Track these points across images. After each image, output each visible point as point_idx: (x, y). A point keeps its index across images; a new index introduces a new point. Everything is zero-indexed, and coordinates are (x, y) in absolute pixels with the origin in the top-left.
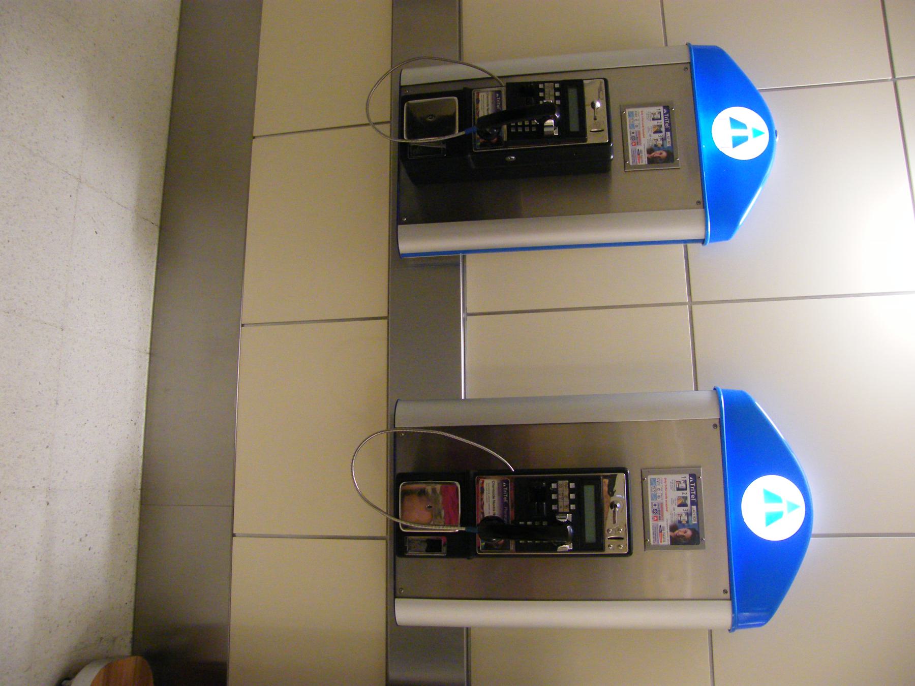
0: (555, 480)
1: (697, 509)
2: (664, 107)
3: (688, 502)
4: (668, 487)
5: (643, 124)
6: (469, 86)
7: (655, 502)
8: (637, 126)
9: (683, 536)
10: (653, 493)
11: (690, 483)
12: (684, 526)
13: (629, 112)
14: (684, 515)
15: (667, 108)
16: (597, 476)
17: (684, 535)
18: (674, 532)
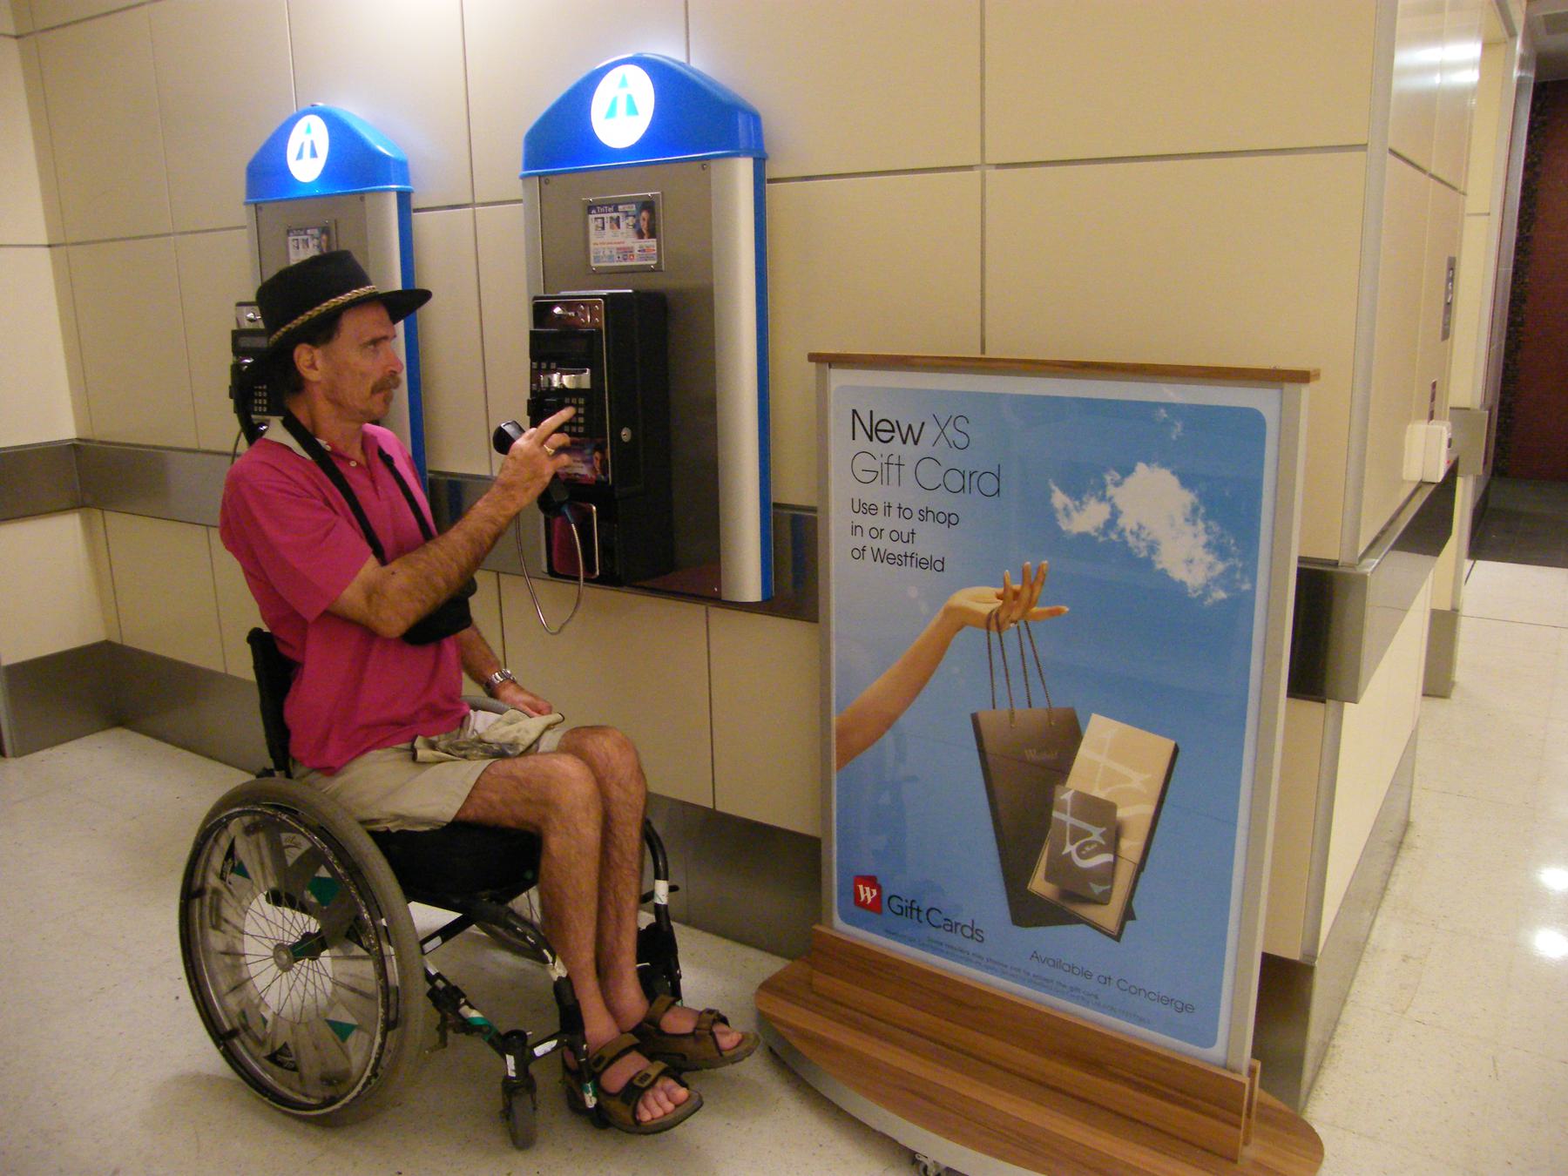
1: (622, 204)
3: (615, 215)
11: (597, 213)
12: (638, 221)
14: (627, 221)
15: (288, 232)
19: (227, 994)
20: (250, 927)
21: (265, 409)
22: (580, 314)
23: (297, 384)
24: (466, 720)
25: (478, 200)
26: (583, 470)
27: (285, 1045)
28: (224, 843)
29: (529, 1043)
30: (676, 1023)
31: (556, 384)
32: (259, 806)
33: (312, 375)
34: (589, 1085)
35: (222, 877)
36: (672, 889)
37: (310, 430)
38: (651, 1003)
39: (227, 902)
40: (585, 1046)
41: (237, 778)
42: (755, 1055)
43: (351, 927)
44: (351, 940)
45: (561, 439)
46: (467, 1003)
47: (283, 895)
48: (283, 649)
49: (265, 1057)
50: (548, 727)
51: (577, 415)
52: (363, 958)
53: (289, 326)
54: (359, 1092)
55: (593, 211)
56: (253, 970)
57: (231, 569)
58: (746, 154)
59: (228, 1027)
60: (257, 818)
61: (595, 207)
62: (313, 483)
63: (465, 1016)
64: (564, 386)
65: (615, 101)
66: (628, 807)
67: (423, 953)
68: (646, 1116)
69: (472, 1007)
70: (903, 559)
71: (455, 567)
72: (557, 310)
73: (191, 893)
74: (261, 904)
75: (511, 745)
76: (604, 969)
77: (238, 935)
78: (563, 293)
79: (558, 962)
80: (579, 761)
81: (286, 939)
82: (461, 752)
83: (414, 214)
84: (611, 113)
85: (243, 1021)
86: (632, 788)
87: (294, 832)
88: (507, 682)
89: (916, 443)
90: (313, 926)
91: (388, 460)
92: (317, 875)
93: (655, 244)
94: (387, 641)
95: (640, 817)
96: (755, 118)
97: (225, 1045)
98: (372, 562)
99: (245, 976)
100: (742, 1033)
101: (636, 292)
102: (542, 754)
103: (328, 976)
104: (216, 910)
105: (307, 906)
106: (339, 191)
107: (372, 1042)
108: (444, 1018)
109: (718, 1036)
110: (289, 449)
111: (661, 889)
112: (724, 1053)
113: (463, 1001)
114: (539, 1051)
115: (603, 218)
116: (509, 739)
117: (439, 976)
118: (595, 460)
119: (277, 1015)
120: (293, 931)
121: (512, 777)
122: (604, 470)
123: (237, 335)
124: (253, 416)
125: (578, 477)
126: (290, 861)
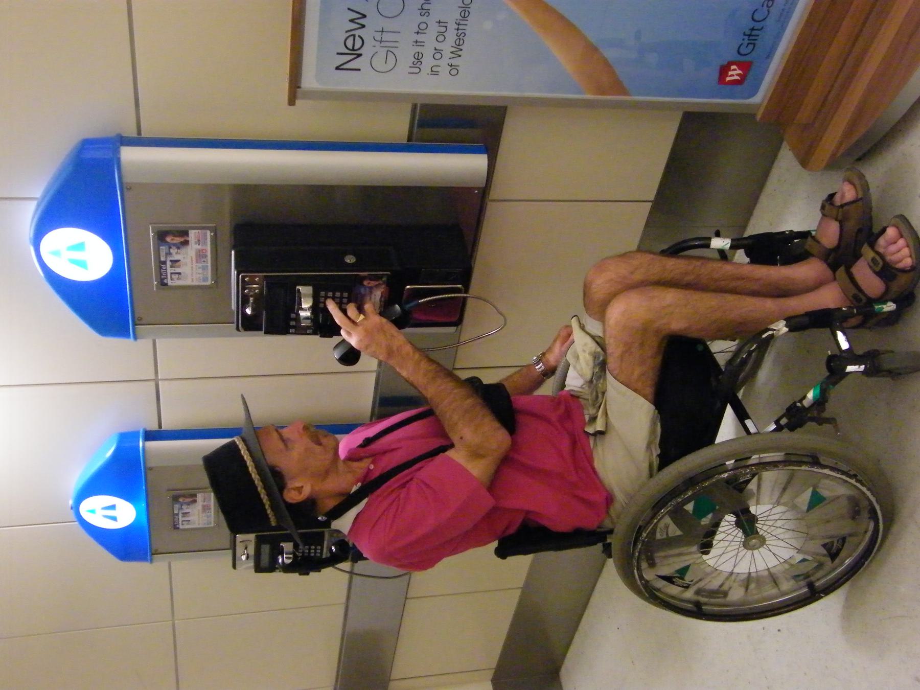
1: (160, 258)
2: (166, 284)
3: (169, 264)
5: (192, 270)
6: (379, 420)
7: (205, 264)
8: (199, 268)
11: (166, 278)
12: (175, 245)
13: (208, 281)
14: (174, 254)
15: (176, 527)
16: (262, 328)
17: (173, 238)
19: (779, 589)
20: (727, 568)
21: (319, 547)
22: (251, 294)
23: (311, 503)
24: (572, 393)
25: (153, 377)
26: (378, 294)
27: (824, 546)
28: (661, 584)
29: (838, 353)
30: (830, 235)
31: (308, 314)
32: (633, 554)
33: (307, 491)
34: (876, 307)
35: (687, 587)
36: (718, 234)
37: (345, 497)
38: (813, 256)
39: (706, 585)
40: (844, 309)
41: (611, 567)
42: (863, 171)
43: (735, 488)
44: (744, 488)
45: (352, 310)
46: (801, 401)
47: (705, 540)
48: (512, 531)
49: (832, 562)
50: (582, 328)
51: (334, 298)
52: (760, 479)
53: (267, 507)
54: (869, 489)
55: (165, 281)
56: (761, 566)
57: (449, 565)
58: (117, 152)
59: (806, 590)
60: (643, 557)
61: (162, 280)
62: (389, 494)
63: (812, 402)
64: (311, 307)
65: (74, 262)
66: (651, 266)
67: (758, 433)
68: (908, 262)
69: (805, 397)
70: (460, 32)
71: (455, 391)
72: (249, 311)
73: (698, 612)
74: (710, 559)
75: (595, 358)
76: (781, 292)
77: (733, 577)
78: (234, 307)
79: (772, 326)
80: (611, 303)
81: (739, 540)
82: (599, 397)
83: (164, 428)
84: (82, 264)
85: (801, 578)
86: (635, 262)
87: (656, 528)
88: (544, 360)
89: (364, 16)
90: (730, 518)
91: (368, 442)
92: (691, 512)
93: (193, 231)
94: (514, 447)
95: (659, 257)
96: (87, 144)
97: (820, 592)
98: (451, 453)
99: (766, 573)
100: (843, 182)
101: (234, 247)
102: (604, 331)
103: (771, 509)
104: (713, 593)
105: (714, 522)
106: (144, 487)
107: (828, 477)
108: (812, 419)
109: (845, 202)
110: (358, 515)
111: (718, 243)
112: (860, 196)
113: (799, 404)
114: (844, 345)
115: (172, 273)
116: (589, 358)
117: (777, 422)
118: (370, 285)
119: (799, 551)
120: (734, 533)
121: (622, 357)
122: (377, 278)
123: (259, 569)
124: (324, 556)
125: (383, 299)
126: (679, 533)
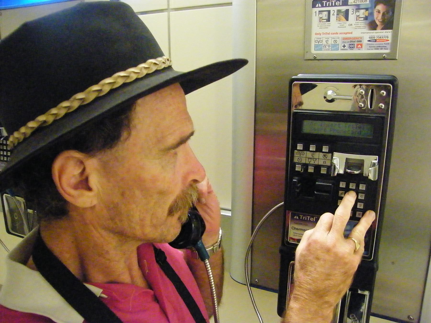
0: (293, 165)
3: (344, 8)
4: (325, 31)
7: (341, 47)
9: (383, 15)
10: (330, 48)
11: (322, 6)
12: (371, 14)
14: (357, 14)
17: (382, 13)
18: (377, 26)
25: (172, 7)
51: (357, 201)
115: (329, 12)
